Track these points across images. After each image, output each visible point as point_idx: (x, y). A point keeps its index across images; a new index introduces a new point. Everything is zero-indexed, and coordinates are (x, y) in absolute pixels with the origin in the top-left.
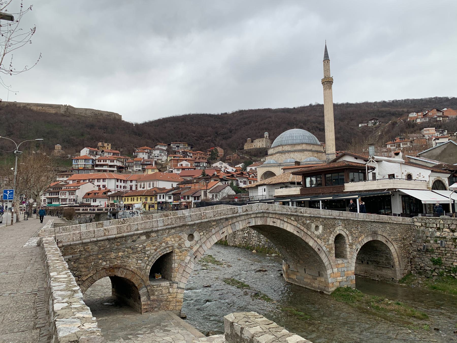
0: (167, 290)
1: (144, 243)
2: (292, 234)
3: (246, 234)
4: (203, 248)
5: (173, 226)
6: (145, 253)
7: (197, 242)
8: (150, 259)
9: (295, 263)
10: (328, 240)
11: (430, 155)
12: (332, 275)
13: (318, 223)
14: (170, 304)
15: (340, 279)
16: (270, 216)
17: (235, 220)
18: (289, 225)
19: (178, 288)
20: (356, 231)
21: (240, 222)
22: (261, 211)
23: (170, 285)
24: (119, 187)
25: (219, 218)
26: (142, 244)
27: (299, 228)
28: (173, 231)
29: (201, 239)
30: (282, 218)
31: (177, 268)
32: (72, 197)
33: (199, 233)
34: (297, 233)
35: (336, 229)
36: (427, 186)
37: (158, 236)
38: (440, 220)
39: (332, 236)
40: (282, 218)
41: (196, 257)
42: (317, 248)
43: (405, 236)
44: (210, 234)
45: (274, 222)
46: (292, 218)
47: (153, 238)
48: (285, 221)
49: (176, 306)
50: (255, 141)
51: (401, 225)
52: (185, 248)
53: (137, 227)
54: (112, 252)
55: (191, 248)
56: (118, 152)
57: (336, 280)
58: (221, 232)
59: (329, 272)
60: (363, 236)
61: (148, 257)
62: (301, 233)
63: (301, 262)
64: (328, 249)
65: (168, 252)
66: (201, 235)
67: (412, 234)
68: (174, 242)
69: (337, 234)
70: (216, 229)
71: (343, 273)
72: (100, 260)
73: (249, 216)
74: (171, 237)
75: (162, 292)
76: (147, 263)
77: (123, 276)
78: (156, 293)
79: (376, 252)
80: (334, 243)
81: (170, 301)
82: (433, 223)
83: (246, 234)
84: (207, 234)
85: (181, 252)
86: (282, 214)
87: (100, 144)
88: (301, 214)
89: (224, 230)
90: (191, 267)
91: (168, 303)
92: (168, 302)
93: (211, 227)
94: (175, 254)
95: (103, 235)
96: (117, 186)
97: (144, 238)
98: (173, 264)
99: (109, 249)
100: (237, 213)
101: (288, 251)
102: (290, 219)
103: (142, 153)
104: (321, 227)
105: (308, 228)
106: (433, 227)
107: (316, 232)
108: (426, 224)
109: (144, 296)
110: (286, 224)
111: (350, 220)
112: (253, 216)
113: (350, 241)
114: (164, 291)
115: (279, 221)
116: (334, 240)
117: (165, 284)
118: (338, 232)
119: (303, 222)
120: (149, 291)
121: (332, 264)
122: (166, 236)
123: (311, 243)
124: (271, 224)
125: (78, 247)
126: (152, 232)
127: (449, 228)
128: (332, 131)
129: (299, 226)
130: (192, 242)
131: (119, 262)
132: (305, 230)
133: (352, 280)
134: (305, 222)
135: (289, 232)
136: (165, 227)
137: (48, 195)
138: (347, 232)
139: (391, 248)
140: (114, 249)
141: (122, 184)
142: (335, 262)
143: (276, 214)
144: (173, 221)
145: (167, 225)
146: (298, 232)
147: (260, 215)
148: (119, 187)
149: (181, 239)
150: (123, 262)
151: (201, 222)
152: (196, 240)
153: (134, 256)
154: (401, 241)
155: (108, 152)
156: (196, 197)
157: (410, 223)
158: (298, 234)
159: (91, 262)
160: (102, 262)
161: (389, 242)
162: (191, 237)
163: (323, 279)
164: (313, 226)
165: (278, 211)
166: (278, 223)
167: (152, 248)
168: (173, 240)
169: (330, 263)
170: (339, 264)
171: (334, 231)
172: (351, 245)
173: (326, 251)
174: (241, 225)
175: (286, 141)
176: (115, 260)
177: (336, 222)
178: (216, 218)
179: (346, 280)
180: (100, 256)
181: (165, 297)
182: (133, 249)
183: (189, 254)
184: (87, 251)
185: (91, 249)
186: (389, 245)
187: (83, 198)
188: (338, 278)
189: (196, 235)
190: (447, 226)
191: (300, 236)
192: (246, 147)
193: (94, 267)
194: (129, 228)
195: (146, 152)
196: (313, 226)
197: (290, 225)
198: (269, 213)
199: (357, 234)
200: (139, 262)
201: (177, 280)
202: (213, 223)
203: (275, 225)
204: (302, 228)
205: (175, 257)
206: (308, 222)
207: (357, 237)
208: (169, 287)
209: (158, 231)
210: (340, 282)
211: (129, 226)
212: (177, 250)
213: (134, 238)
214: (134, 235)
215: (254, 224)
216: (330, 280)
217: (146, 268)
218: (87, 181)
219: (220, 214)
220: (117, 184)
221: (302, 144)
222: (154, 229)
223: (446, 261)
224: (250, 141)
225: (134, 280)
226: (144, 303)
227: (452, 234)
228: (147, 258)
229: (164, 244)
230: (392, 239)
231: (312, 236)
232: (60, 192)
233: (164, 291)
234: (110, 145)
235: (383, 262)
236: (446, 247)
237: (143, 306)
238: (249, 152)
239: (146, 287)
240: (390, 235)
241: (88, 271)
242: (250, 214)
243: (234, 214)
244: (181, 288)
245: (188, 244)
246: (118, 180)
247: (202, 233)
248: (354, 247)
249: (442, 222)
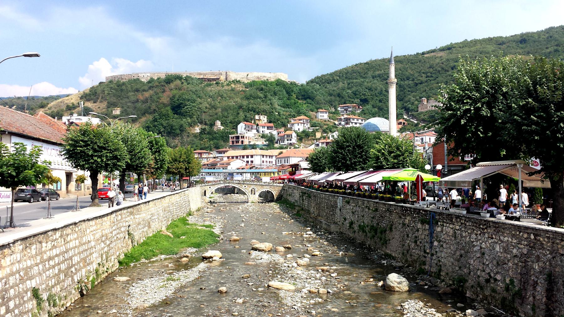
56: (272, 125)
87: (257, 117)
96: (263, 162)
141: (268, 159)
148: (265, 162)
155: (263, 126)
162: (210, 187)
195: (301, 123)
220: (263, 159)
234: (266, 117)
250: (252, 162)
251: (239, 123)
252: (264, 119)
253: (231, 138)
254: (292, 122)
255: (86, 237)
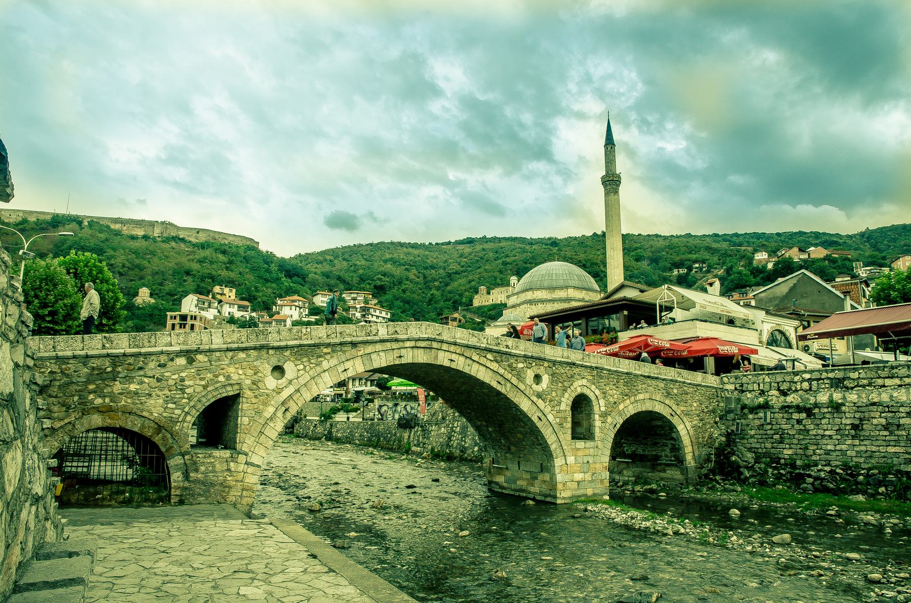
0: (225, 464)
1: (182, 371)
2: (489, 387)
3: (443, 428)
4: (304, 395)
5: (241, 345)
6: (183, 391)
7: (290, 382)
8: (192, 404)
9: (503, 454)
10: (560, 403)
11: (770, 296)
12: (565, 468)
13: (541, 371)
14: (229, 491)
15: (578, 476)
16: (445, 346)
17: (370, 349)
18: (482, 369)
19: (247, 463)
20: (614, 392)
21: (382, 354)
22: (426, 336)
23: (232, 457)
25: (337, 341)
26: (179, 374)
27: (502, 376)
28: (242, 355)
29: (298, 377)
30: (467, 354)
31: (248, 427)
33: (296, 365)
34: (499, 385)
35: (576, 384)
36: (759, 339)
37: (210, 361)
38: (764, 376)
39: (566, 395)
40: (467, 354)
41: (286, 410)
42: (536, 417)
43: (707, 407)
44: (318, 369)
45: (452, 360)
46: (489, 356)
47: (200, 365)
48: (474, 361)
49: (241, 497)
50: (493, 291)
51: (699, 388)
52: (266, 391)
53: (169, 339)
54: (116, 381)
55: (279, 391)
56: (246, 303)
57: (571, 478)
58: (341, 369)
59: (558, 462)
60: (628, 401)
61: (188, 399)
62: (505, 385)
63: (513, 449)
64: (558, 420)
65: (231, 393)
66: (299, 370)
67: (718, 405)
68: (243, 377)
69: (576, 394)
70: (331, 361)
71: (586, 466)
72: (90, 393)
73: (401, 344)
74: (237, 366)
75: (214, 467)
76: (186, 410)
77: (136, 429)
78: (203, 468)
79: (656, 439)
80: (572, 409)
81: (230, 487)
82: (754, 383)
83: (443, 428)
84: (311, 369)
85: (256, 397)
86: (467, 346)
87: (217, 289)
88: (507, 350)
89: (348, 365)
90: (276, 428)
91: (227, 489)
92: (225, 487)
93: (320, 356)
94: (244, 400)
95: (100, 346)
97: (182, 361)
98: (239, 418)
99: (111, 376)
100: (375, 335)
101: (490, 429)
102: (485, 357)
103: (289, 307)
104: (546, 379)
105: (520, 376)
106: (753, 391)
107: (534, 386)
108: (742, 386)
109: (177, 470)
110: (475, 366)
111: (603, 369)
112: (408, 344)
113: (603, 409)
114: (218, 467)
115: (462, 359)
116: (570, 403)
117: (222, 454)
118: (579, 390)
119: (509, 366)
120: (188, 462)
121: (564, 448)
122: (226, 363)
123: (525, 405)
124: (447, 363)
125: (48, 364)
126: (198, 351)
127: (779, 390)
128: (618, 267)
129: (501, 371)
130: (280, 382)
131: (129, 401)
132: (514, 381)
133: (602, 481)
134: (515, 365)
135: (483, 383)
136: (225, 346)
138: (597, 392)
139: (680, 428)
140: (120, 376)
142: (571, 445)
143: (455, 344)
144: (243, 337)
145: (230, 343)
146: (499, 383)
147: (423, 344)
149: (258, 372)
150: (138, 402)
151: (300, 346)
152: (289, 378)
153: (160, 393)
154: (698, 416)
155: (230, 304)
156: (374, 380)
157: (716, 386)
158: (499, 388)
159: (73, 396)
160: (95, 398)
161: (677, 416)
162: (279, 370)
163: (547, 477)
165: (460, 338)
166: (459, 362)
167: (198, 382)
168: (241, 372)
169: (561, 446)
170: (578, 449)
171: (572, 387)
172: (604, 415)
173: (553, 423)
174: (384, 359)
175: (539, 283)
176: (121, 396)
177: (576, 370)
178: (332, 341)
179: (590, 479)
180: (92, 387)
181: (221, 478)
182: (159, 380)
183: (272, 403)
184: (65, 374)
185: (75, 371)
186: (675, 421)
188: (576, 475)
189: (290, 368)
190: (776, 385)
191: (503, 391)
192: (477, 302)
193: (79, 406)
194: (153, 340)
196: (530, 374)
197: (484, 368)
198: (442, 342)
199: (616, 396)
200: (171, 406)
201: (245, 448)
202: (325, 350)
203: (453, 366)
204: (509, 376)
205: (245, 406)
206: (520, 365)
207: (615, 403)
208: (229, 460)
209: (211, 351)
210: (578, 482)
211: (153, 337)
212: (248, 393)
213: (163, 359)
214: (162, 353)
215: (410, 361)
216: (559, 478)
217: (184, 421)
219: (341, 333)
221: (567, 287)
222: (202, 347)
223: (773, 448)
224: (485, 292)
225: (157, 439)
226: (176, 484)
227: (783, 398)
228: (187, 401)
229: (221, 378)
230: (683, 411)
231: (527, 392)
233: (217, 466)
234: (234, 290)
235: (666, 456)
236: (773, 423)
237: (173, 490)
238: (480, 311)
239: (183, 455)
240: (678, 405)
241: (66, 411)
242: (403, 341)
243: (369, 336)
244: (252, 465)
245: (271, 382)
247: (301, 367)
248: (609, 419)
249: (767, 379)
251: (186, 294)
253: (171, 318)
254: (279, 302)
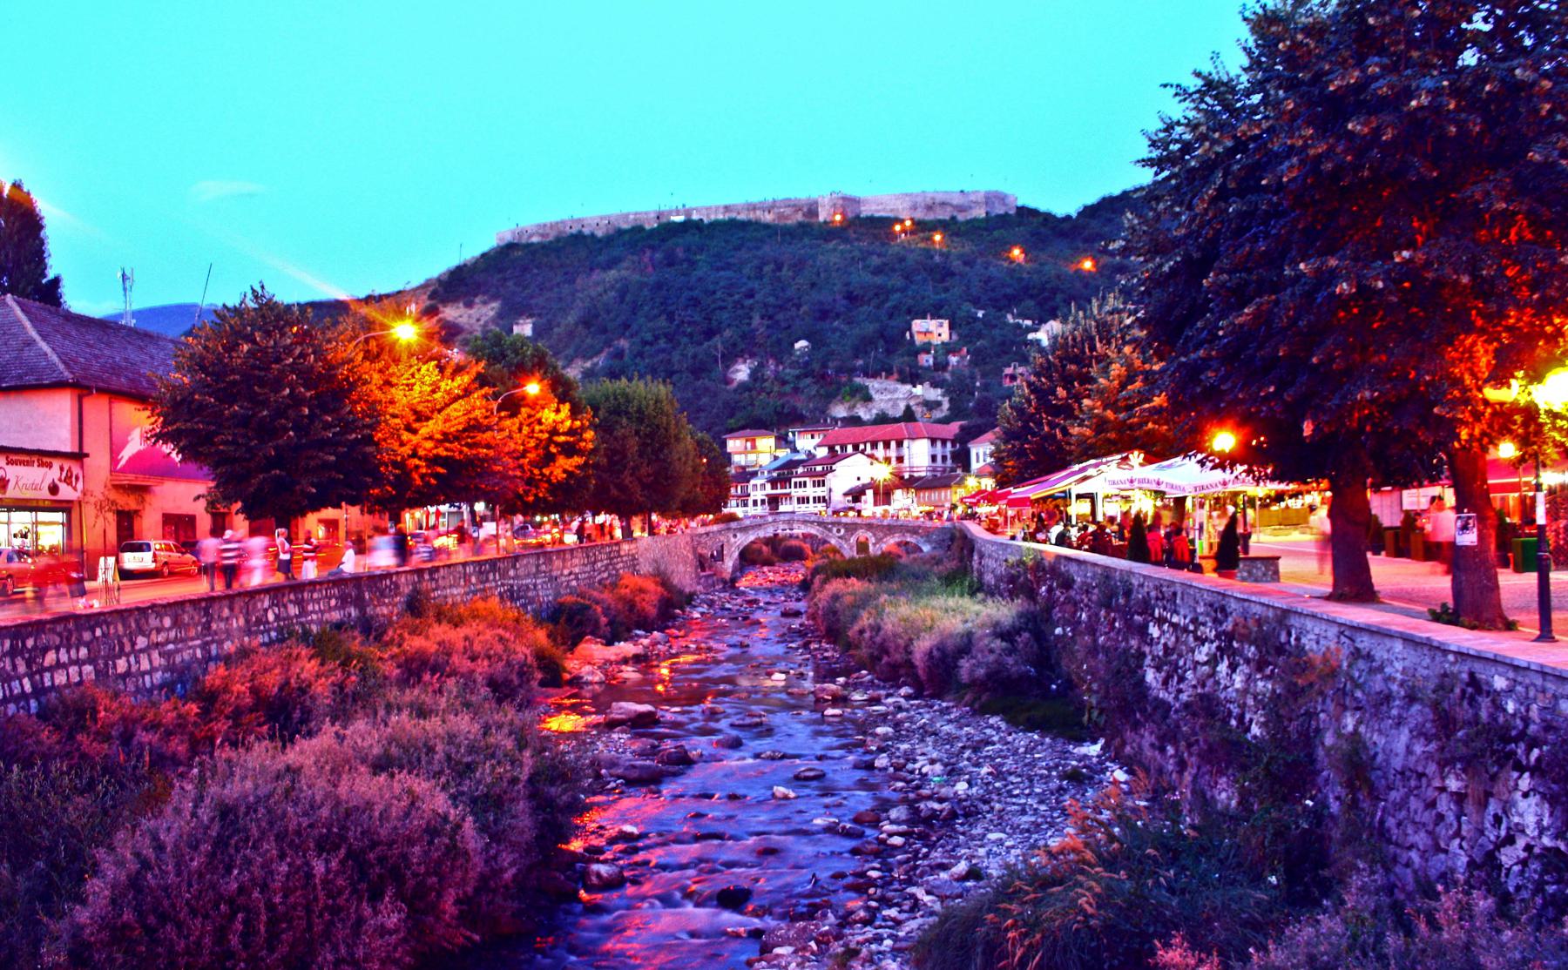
24: (939, 459)
32: (820, 492)
96: (934, 458)
104: (842, 531)
105: (830, 530)
137: (769, 490)
148: (939, 459)
164: (835, 530)
187: (846, 494)
196: (835, 530)
218: (850, 449)
232: (793, 480)
234: (946, 323)
245: (733, 540)
246: (933, 441)
250: (900, 459)
252: (940, 330)
255: (132, 659)
